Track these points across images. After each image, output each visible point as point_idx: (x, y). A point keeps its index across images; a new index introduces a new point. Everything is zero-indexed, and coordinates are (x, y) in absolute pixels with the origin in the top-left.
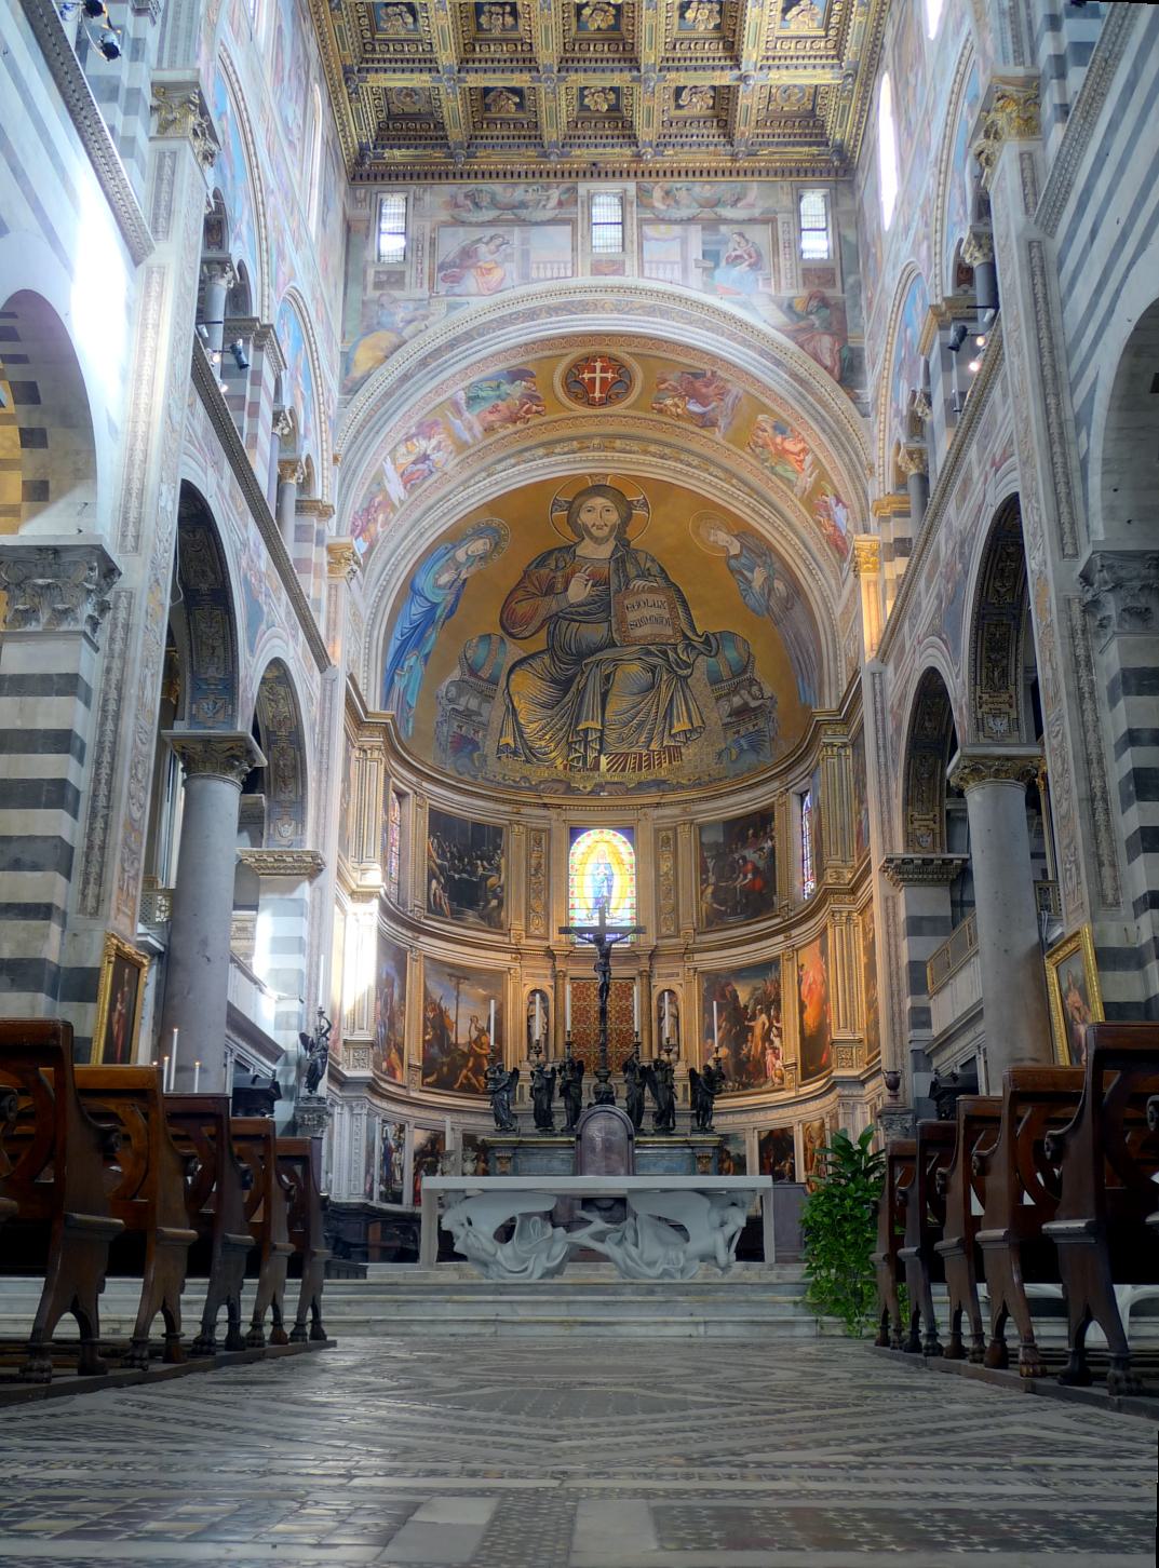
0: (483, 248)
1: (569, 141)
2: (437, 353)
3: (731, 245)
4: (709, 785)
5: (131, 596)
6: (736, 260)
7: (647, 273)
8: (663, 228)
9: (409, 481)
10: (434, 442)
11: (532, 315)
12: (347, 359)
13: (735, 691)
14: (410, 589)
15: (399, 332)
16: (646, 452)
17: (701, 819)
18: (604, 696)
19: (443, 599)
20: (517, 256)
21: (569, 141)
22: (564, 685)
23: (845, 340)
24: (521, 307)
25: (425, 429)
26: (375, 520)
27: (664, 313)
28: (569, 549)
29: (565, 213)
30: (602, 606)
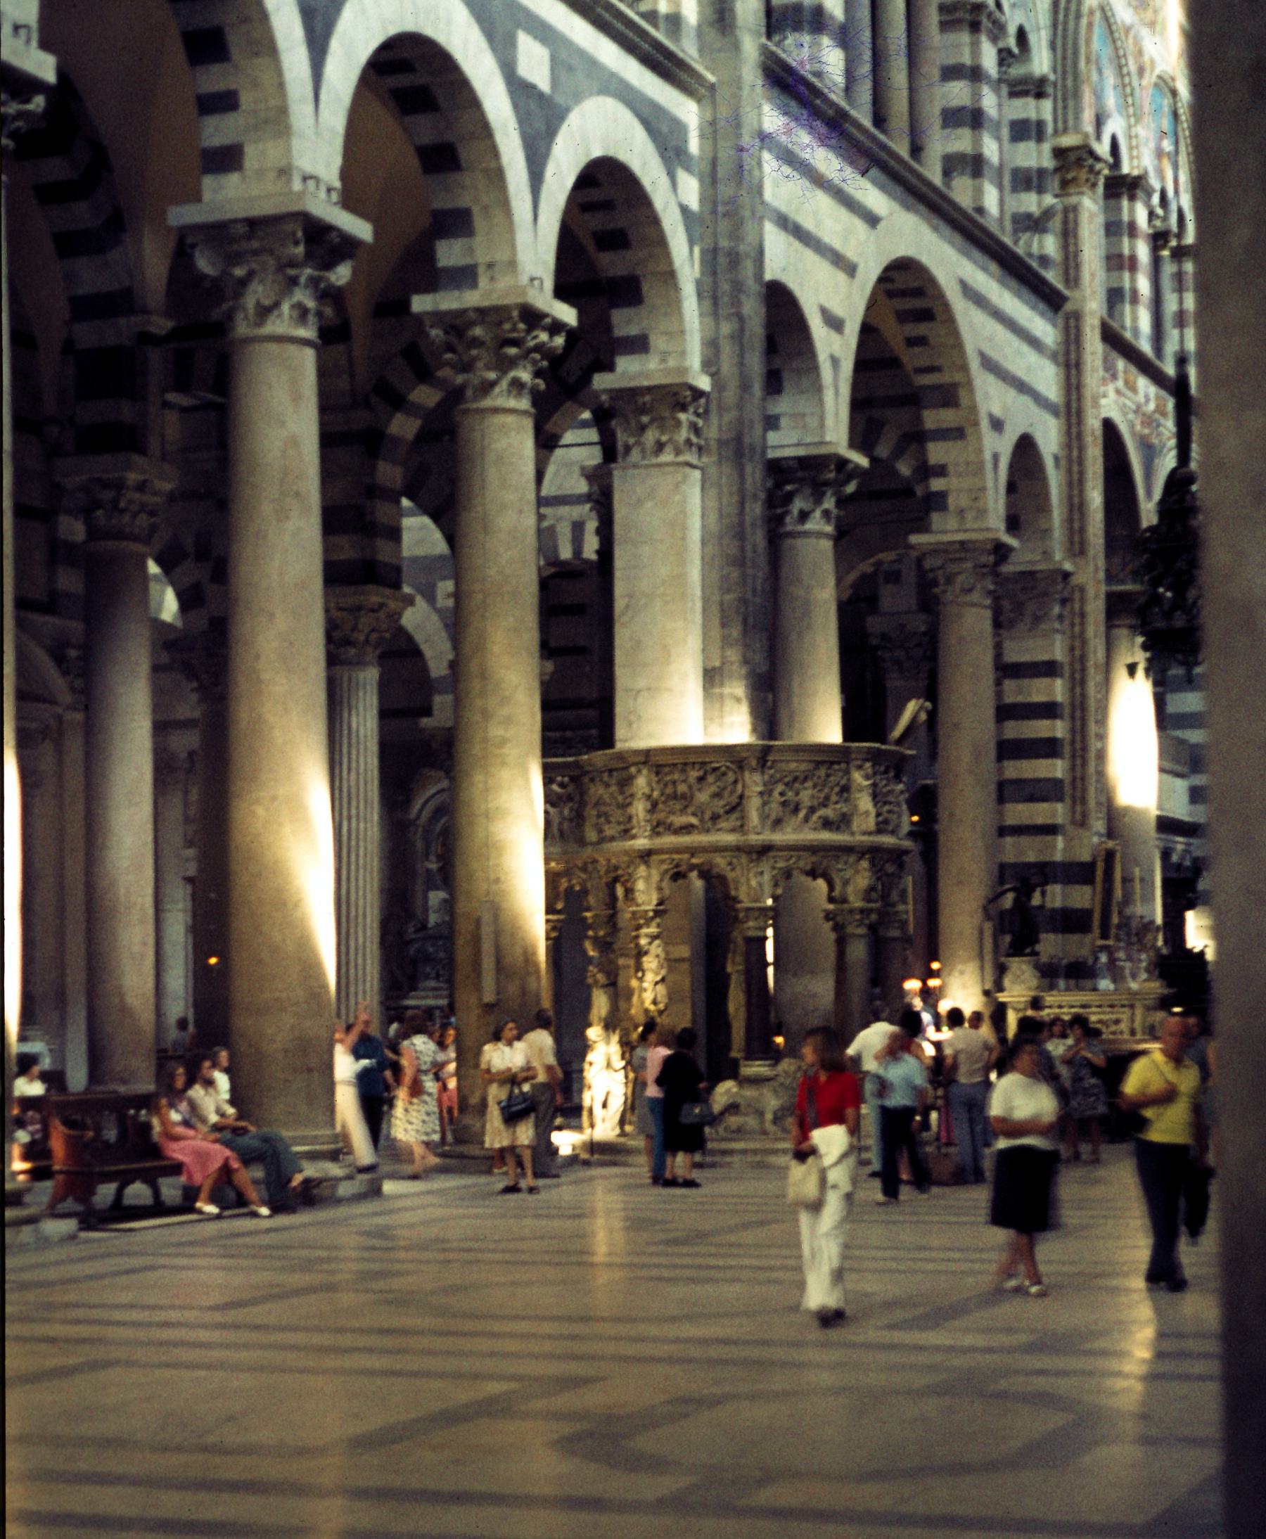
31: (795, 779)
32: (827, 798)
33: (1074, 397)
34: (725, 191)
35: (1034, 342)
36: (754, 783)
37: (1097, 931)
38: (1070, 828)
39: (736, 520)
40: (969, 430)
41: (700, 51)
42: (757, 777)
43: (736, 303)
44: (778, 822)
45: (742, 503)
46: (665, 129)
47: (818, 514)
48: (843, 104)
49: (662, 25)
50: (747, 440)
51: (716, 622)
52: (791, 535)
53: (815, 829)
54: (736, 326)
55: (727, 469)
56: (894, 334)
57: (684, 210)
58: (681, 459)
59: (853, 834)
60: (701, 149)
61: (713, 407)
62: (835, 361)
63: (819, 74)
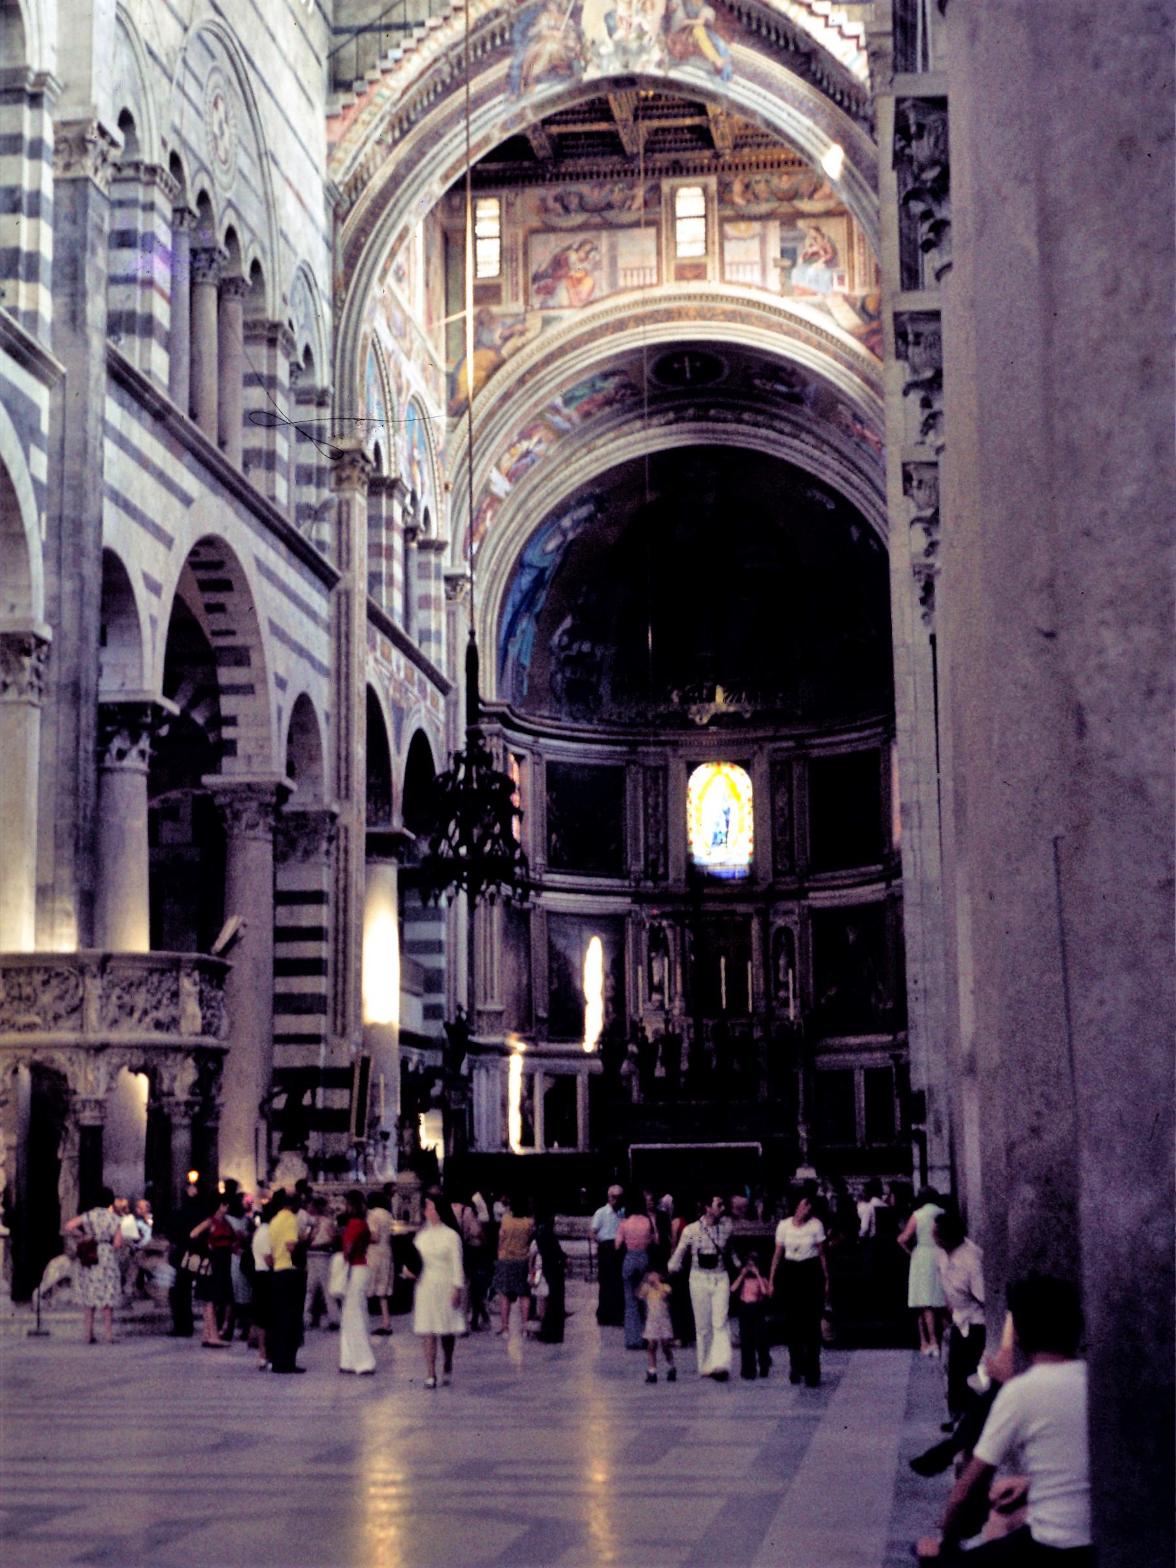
0: (573, 257)
3: (808, 241)
5: (346, 830)
6: (811, 258)
7: (728, 276)
8: (743, 226)
9: (512, 476)
10: (535, 439)
14: (520, 565)
15: (497, 349)
16: (740, 421)
20: (605, 262)
24: (610, 319)
25: (525, 435)
26: (484, 520)
27: (744, 318)
31: (131, 985)
32: (159, 1002)
33: (344, 662)
34: (71, 466)
35: (312, 615)
36: (94, 987)
37: (353, 1130)
38: (330, 1037)
39: (71, 753)
40: (258, 687)
41: (54, 344)
42: (98, 982)
43: (77, 563)
44: (115, 1022)
45: (77, 738)
46: (22, 409)
47: (134, 753)
48: (166, 397)
49: (21, 317)
50: (83, 684)
51: (50, 844)
52: (111, 770)
53: (148, 1029)
54: (77, 583)
55: (65, 708)
56: (197, 601)
57: (35, 481)
58: (24, 698)
59: (180, 1034)
60: (51, 426)
61: (54, 658)
62: (153, 621)
63: (148, 372)
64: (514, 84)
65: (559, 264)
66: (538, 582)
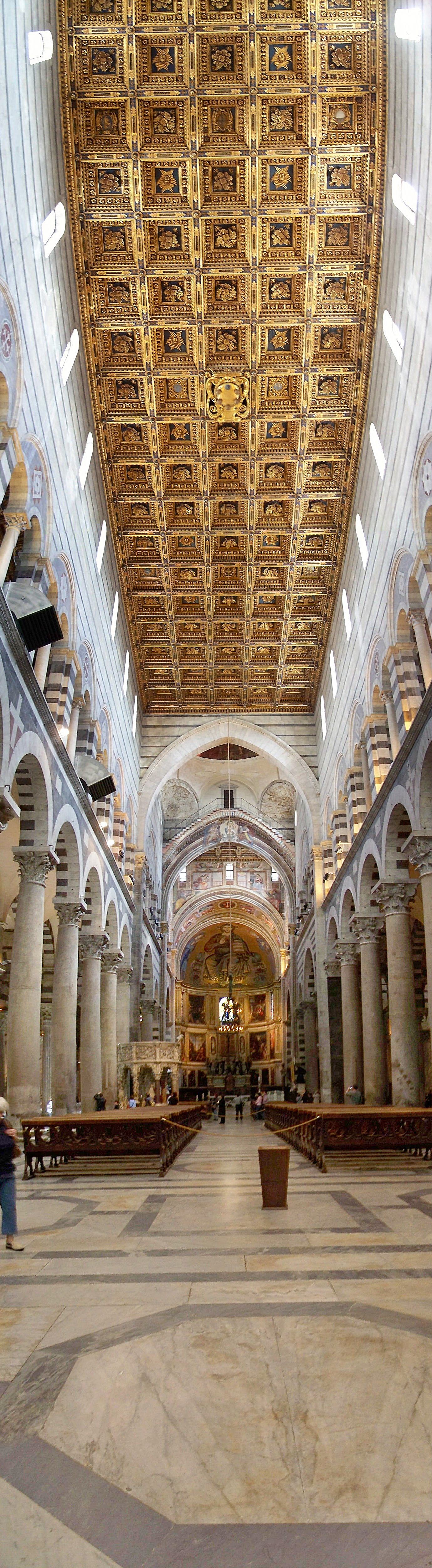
1: (221, 855)
2: (193, 904)
4: (252, 987)
6: (257, 881)
9: (186, 928)
11: (213, 894)
12: (174, 904)
13: (258, 965)
14: (186, 948)
17: (250, 994)
18: (228, 964)
19: (191, 948)
21: (221, 855)
22: (218, 961)
23: (279, 901)
25: (190, 919)
27: (242, 894)
28: (220, 935)
29: (220, 869)
30: (227, 945)
64: (205, 843)
65: (200, 879)
66: (189, 952)
